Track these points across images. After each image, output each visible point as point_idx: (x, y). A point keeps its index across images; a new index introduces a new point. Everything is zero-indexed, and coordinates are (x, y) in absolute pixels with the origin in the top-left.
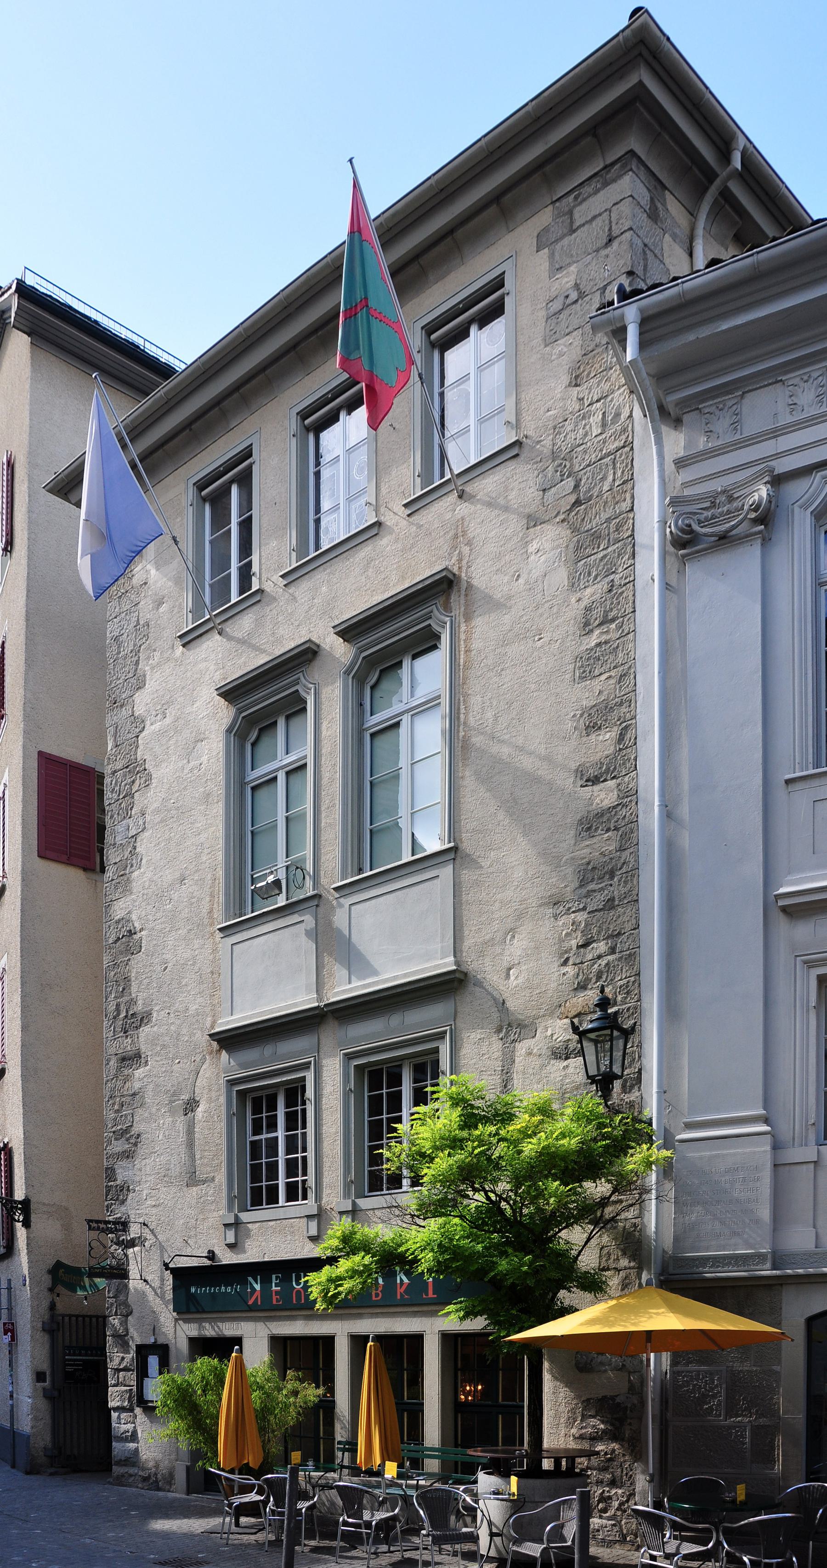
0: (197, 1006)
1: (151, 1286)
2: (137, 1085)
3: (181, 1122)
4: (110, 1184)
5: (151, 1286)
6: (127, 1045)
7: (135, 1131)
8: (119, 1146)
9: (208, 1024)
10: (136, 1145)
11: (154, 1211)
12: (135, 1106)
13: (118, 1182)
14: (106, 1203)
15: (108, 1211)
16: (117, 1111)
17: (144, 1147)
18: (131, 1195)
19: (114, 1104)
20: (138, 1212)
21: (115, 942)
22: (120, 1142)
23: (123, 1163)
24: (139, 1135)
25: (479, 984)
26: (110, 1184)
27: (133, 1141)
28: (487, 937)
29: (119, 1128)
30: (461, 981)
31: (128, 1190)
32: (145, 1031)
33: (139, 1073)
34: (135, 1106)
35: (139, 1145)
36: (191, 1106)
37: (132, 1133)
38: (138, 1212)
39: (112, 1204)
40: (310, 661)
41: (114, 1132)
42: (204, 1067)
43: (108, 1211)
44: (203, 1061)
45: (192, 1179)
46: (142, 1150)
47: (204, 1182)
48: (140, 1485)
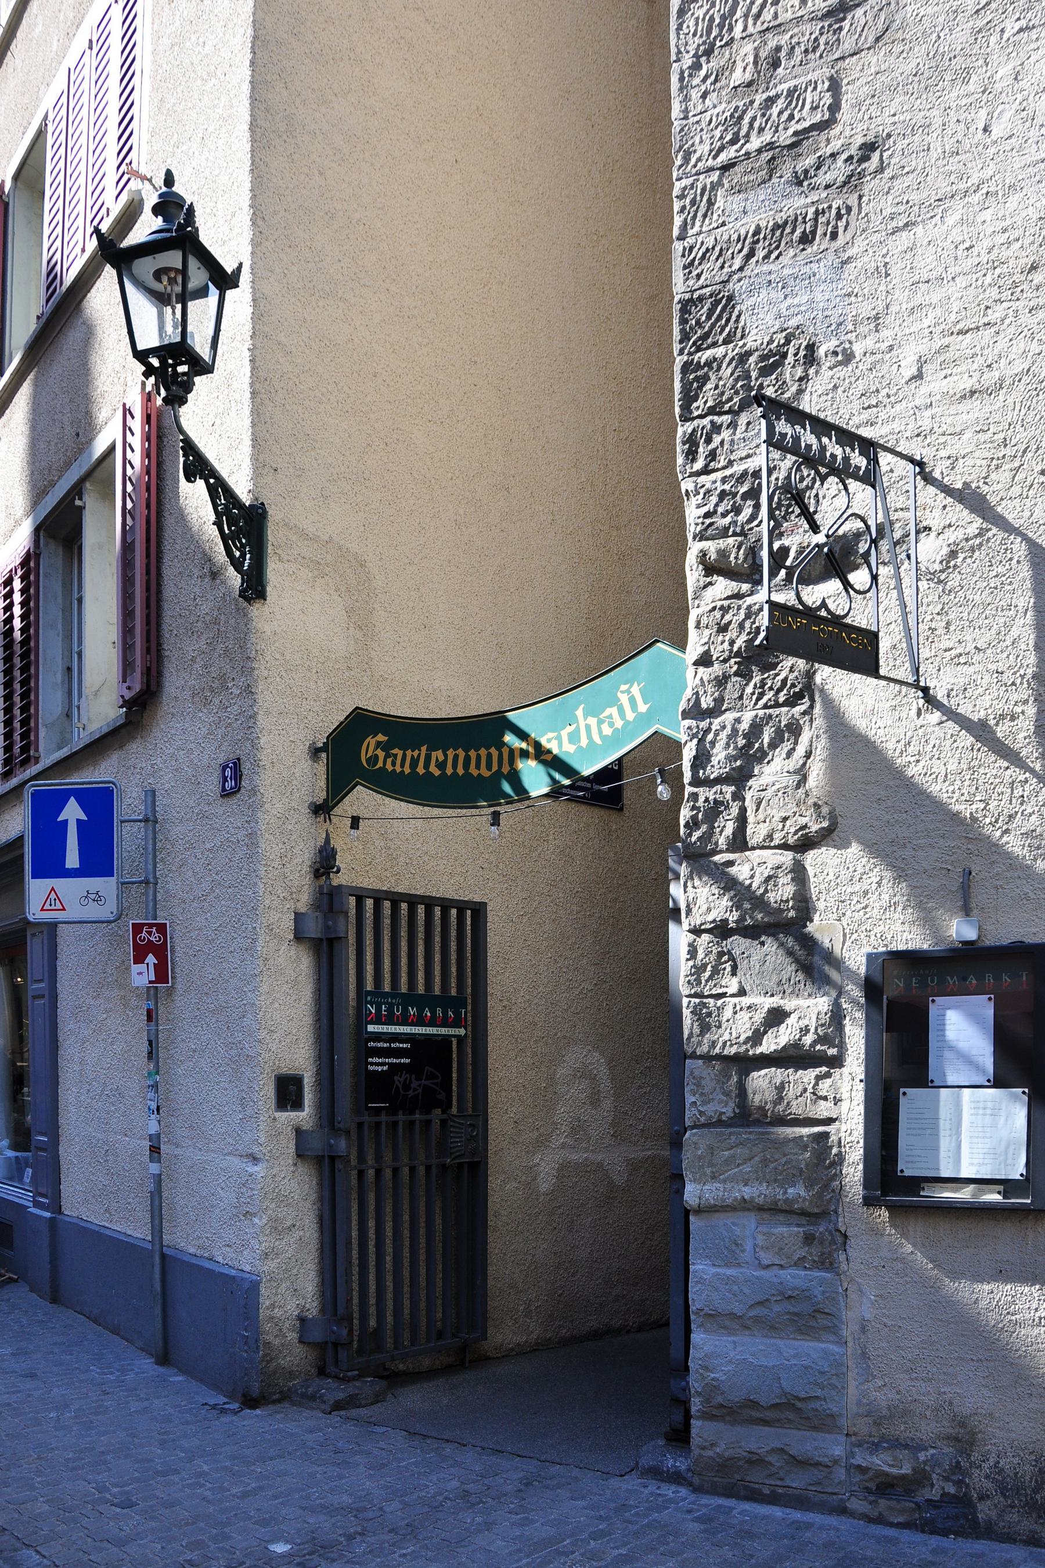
1: (951, 714)
4: (705, 356)
5: (951, 714)
7: (849, 132)
10: (852, 182)
11: (975, 410)
12: (848, 44)
13: (750, 343)
14: (683, 430)
15: (691, 455)
17: (899, 185)
24: (869, 148)
26: (705, 356)
27: (838, 172)
29: (755, 143)
31: (810, 357)
35: (870, 185)
37: (836, 145)
39: (716, 428)
41: (725, 168)
43: (691, 455)
46: (879, 200)
48: (857, 1504)
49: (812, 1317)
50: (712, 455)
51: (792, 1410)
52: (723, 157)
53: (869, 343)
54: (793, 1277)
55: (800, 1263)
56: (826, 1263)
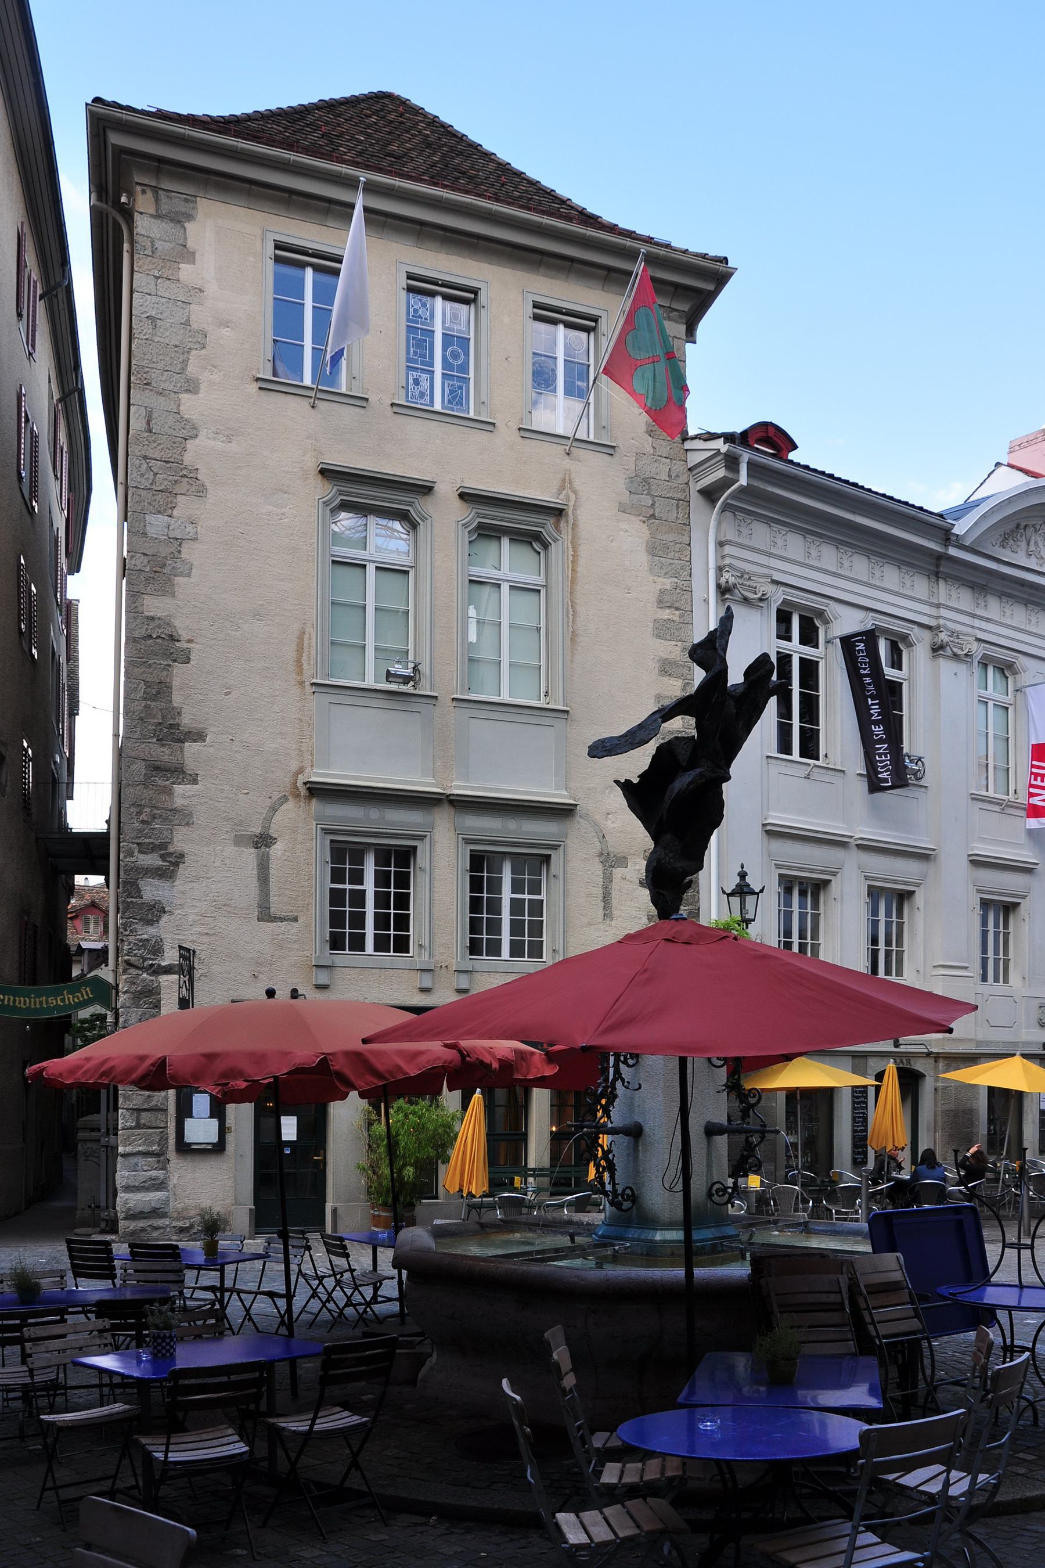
0: (277, 746)
2: (179, 802)
3: (250, 856)
6: (163, 754)
8: (151, 860)
9: (294, 766)
10: (176, 864)
11: (206, 939)
16: (143, 822)
17: (190, 869)
18: (165, 918)
19: (139, 813)
20: (178, 937)
21: (144, 638)
22: (150, 856)
23: (156, 882)
25: (586, 817)
28: (591, 786)
30: (571, 810)
32: (191, 748)
33: (179, 789)
34: (177, 822)
36: (263, 841)
38: (178, 937)
40: (425, 494)
42: (285, 807)
44: (284, 799)
45: (266, 915)
47: (282, 919)
49: (160, 1185)
50: (131, 931)
51: (156, 1213)
52: (137, 841)
53: (179, 911)
54: (154, 1173)
55: (155, 1169)
56: (164, 1168)
